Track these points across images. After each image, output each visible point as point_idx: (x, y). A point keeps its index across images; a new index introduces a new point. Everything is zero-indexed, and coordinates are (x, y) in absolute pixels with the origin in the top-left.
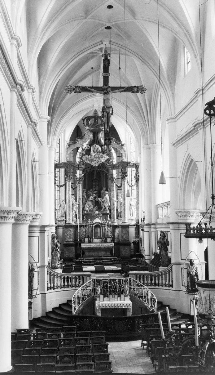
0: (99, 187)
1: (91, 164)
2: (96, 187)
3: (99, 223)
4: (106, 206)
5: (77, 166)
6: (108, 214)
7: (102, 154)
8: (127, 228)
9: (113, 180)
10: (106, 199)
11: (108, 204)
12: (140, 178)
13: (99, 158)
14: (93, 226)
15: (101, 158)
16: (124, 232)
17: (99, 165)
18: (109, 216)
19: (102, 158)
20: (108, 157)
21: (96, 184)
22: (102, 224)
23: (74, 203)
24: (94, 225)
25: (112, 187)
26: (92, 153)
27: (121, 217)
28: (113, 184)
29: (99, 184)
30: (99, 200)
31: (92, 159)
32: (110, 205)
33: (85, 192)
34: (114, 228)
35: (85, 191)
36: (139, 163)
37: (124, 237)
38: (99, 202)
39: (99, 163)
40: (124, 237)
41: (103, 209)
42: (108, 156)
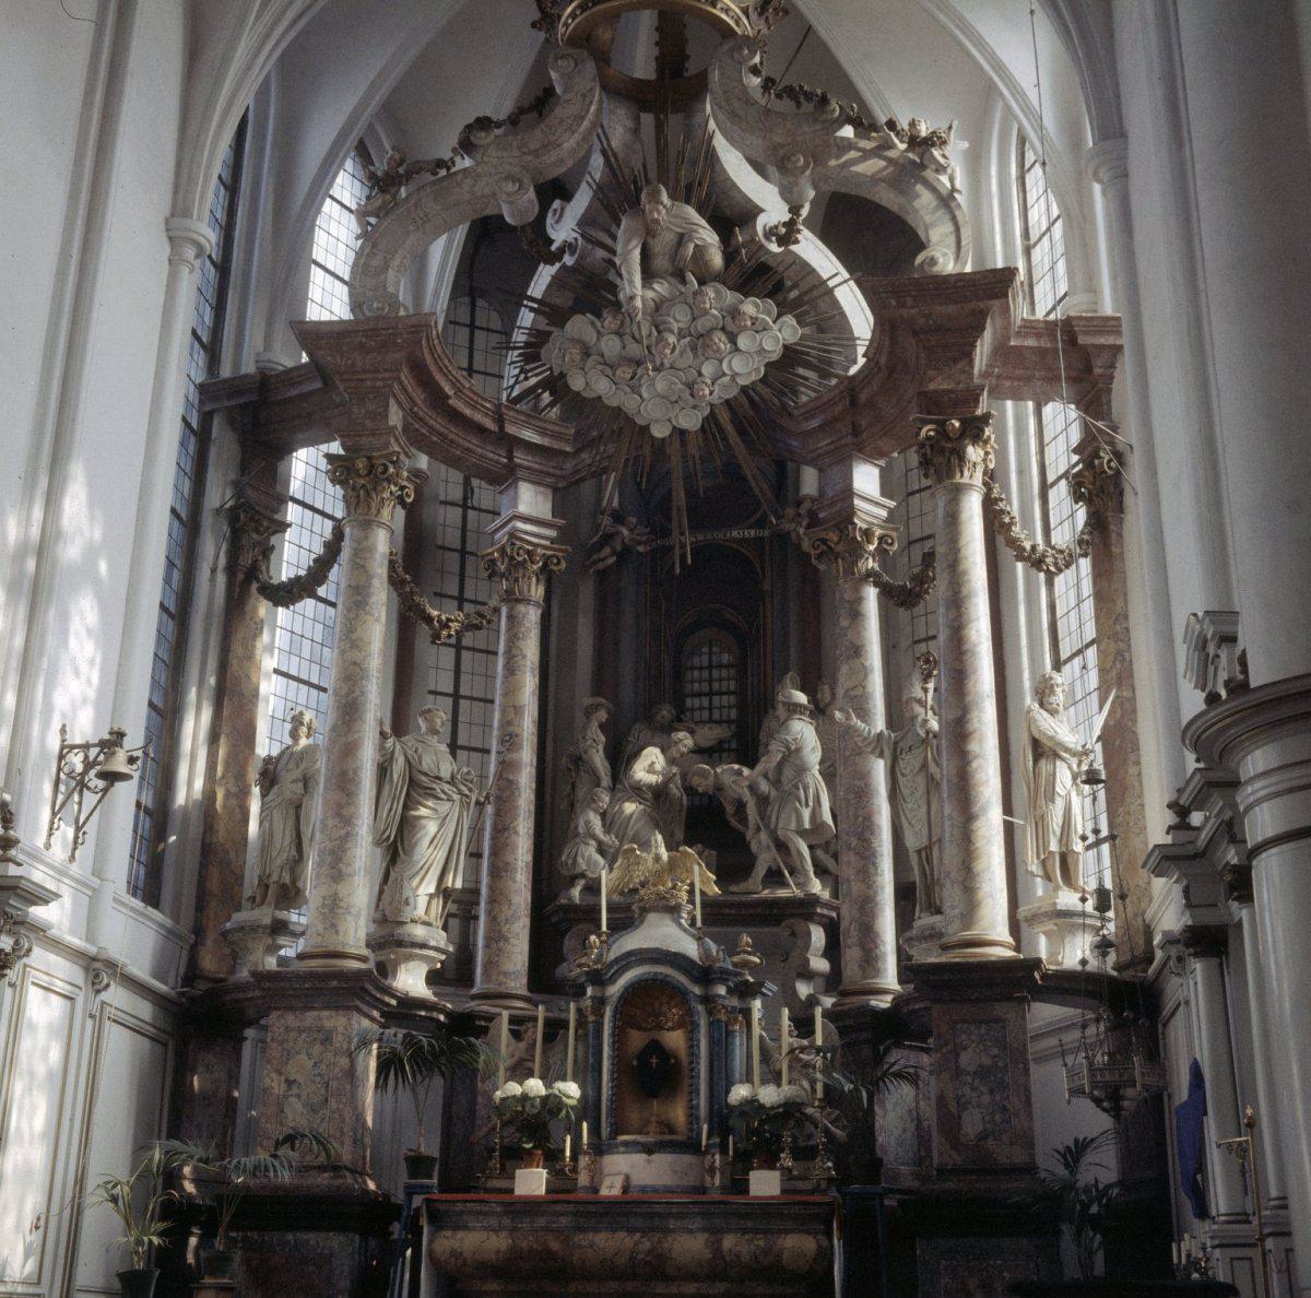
0: (740, 692)
1: (629, 403)
2: (711, 694)
3: (677, 960)
4: (787, 827)
5: (490, 424)
6: (805, 908)
7: (730, 297)
8: (1002, 1009)
9: (856, 550)
10: (792, 754)
11: (806, 814)
12: (1135, 476)
13: (699, 342)
14: (600, 1002)
15: (720, 341)
16: (967, 1060)
17: (711, 419)
18: (818, 936)
19: (732, 339)
20: (786, 331)
21: (711, 662)
22: (705, 974)
23: (427, 763)
24: (615, 989)
25: (844, 623)
26: (635, 289)
27: (939, 911)
28: (857, 590)
29: (741, 667)
30: (719, 788)
31: (634, 350)
32: (827, 817)
33: (601, 726)
34: (866, 1052)
35: (603, 715)
36: (1109, 325)
37: (972, 1124)
38: (730, 809)
39: (714, 393)
40: (972, 1124)
41: (760, 871)
42: (789, 320)
